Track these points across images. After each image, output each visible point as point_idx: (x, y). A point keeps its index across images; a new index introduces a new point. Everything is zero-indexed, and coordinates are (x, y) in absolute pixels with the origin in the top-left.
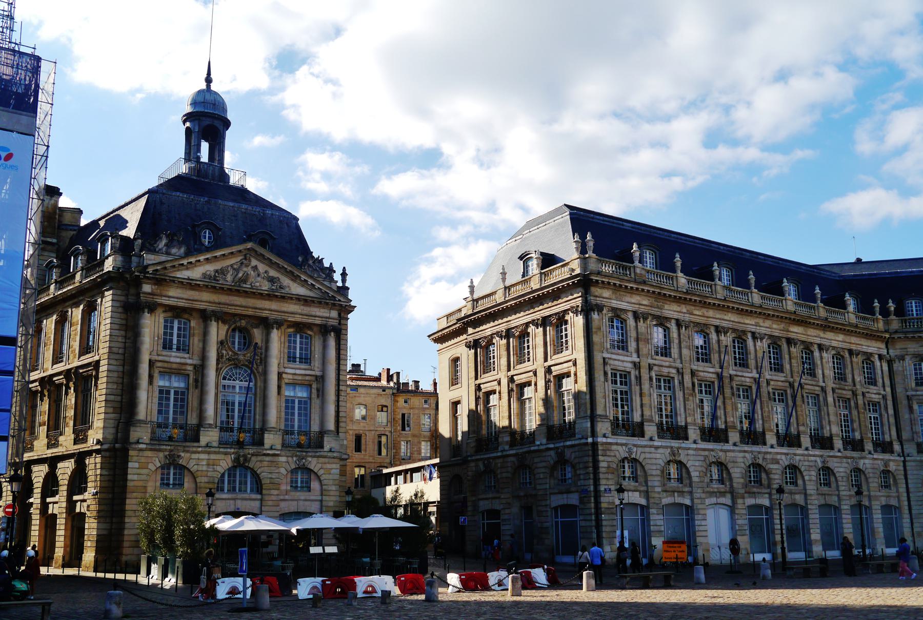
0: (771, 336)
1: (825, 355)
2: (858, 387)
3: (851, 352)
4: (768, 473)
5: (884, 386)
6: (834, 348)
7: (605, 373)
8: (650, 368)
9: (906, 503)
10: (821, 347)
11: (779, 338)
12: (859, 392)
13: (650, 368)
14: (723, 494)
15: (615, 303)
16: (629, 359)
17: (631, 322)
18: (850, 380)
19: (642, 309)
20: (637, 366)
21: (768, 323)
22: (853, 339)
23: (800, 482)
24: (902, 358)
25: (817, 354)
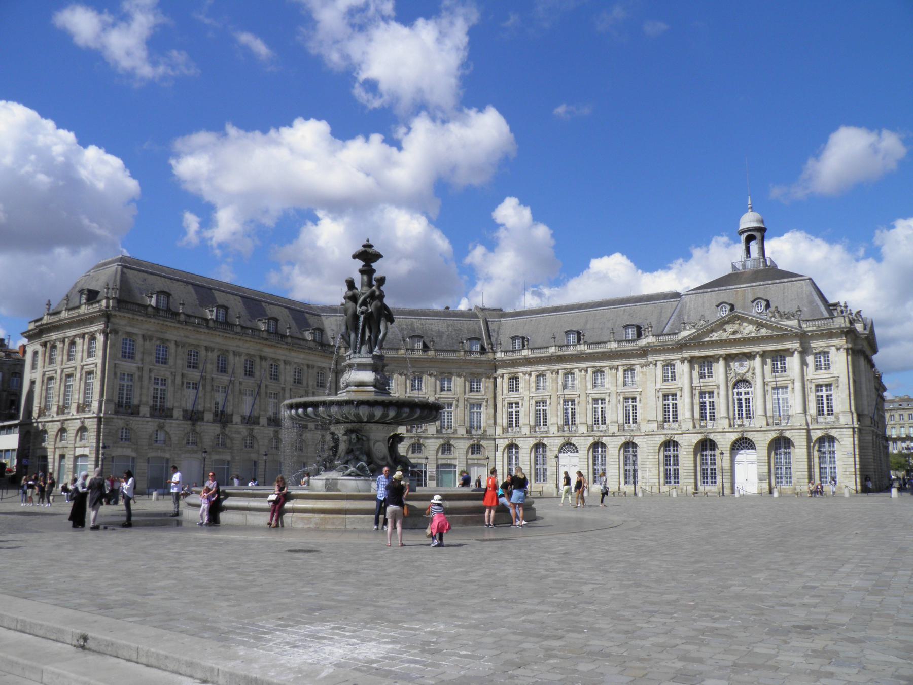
0: (248, 354)
1: (288, 367)
2: (310, 388)
3: (308, 366)
4: (232, 439)
6: (296, 363)
7: (115, 374)
8: (150, 371)
10: (285, 362)
11: (254, 356)
13: (150, 371)
14: (196, 452)
15: (129, 329)
16: (135, 365)
17: (140, 341)
19: (149, 333)
20: (140, 369)
21: (247, 345)
22: (312, 357)
23: (256, 446)
25: (282, 366)
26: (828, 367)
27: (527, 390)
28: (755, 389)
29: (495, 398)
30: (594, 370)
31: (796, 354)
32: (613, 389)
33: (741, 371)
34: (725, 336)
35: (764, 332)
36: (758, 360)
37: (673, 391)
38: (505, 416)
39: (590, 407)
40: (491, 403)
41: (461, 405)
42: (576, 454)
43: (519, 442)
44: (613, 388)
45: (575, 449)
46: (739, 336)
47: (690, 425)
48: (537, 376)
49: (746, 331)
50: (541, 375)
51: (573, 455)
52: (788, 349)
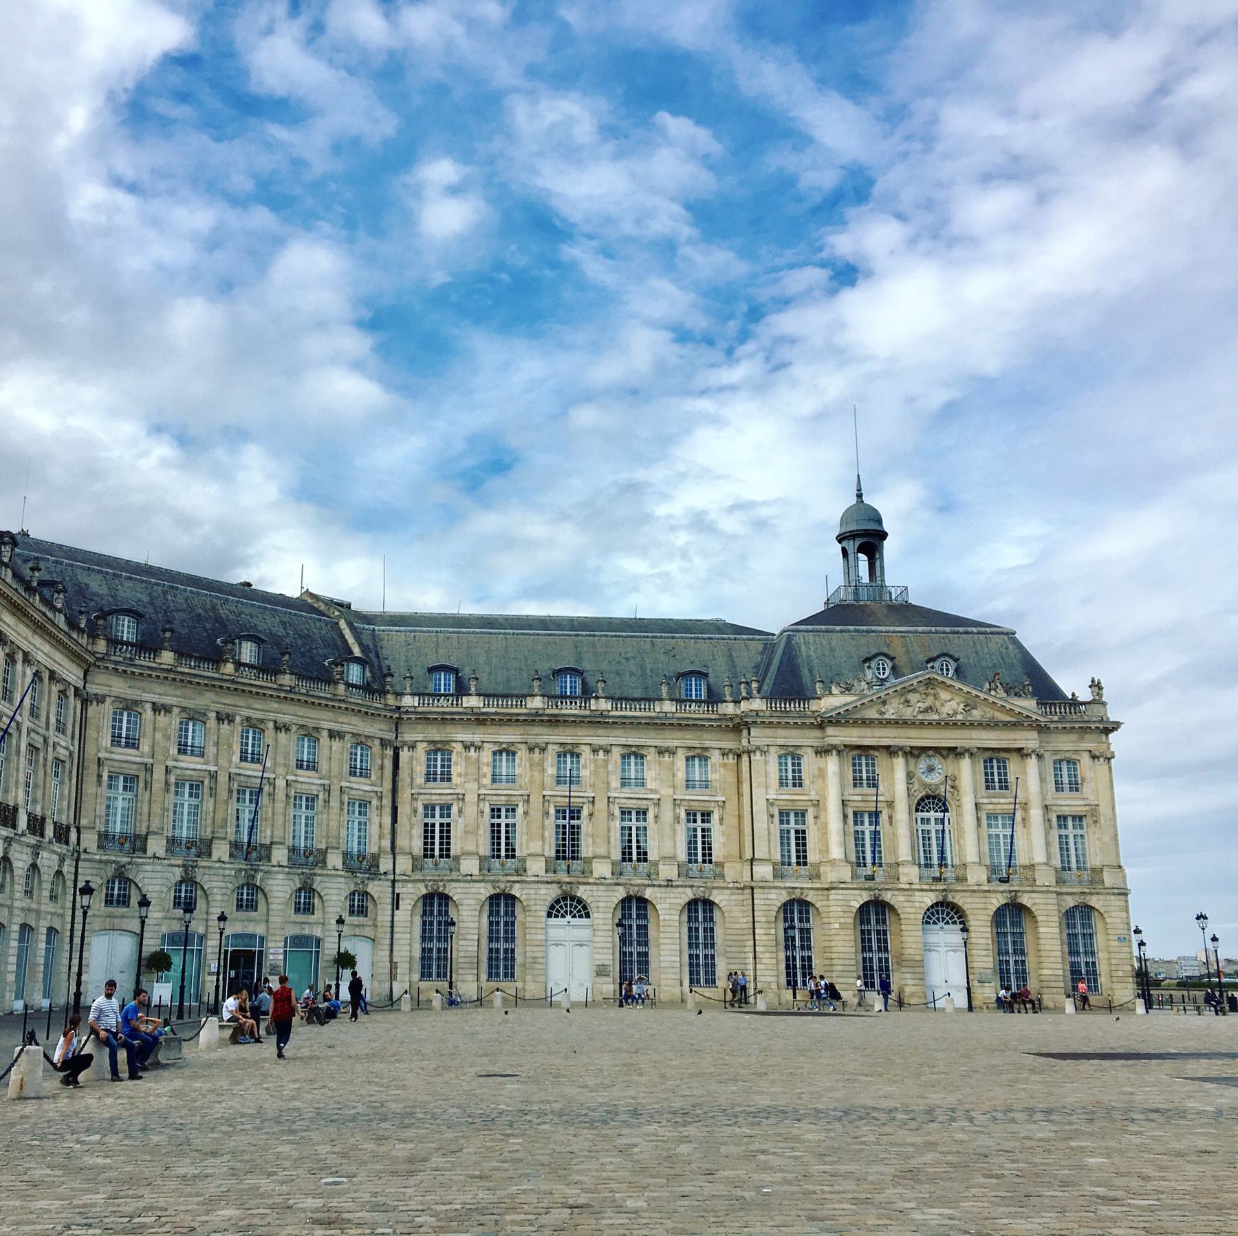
5: (73, 738)
9: (69, 927)
12: (51, 742)
18: (43, 719)
24: (100, 699)
26: (1075, 787)
27: (472, 781)
28: (959, 814)
29: (394, 791)
30: (625, 751)
31: (1032, 762)
32: (666, 792)
33: (935, 779)
34: (908, 713)
35: (976, 714)
36: (966, 763)
37: (800, 806)
38: (418, 832)
39: (617, 824)
40: (387, 802)
41: (334, 803)
42: (584, 921)
43: (454, 891)
44: (666, 792)
45: (582, 910)
46: (936, 717)
47: (845, 873)
48: (494, 753)
49: (947, 709)
50: (508, 751)
51: (577, 921)
52: (1019, 750)
